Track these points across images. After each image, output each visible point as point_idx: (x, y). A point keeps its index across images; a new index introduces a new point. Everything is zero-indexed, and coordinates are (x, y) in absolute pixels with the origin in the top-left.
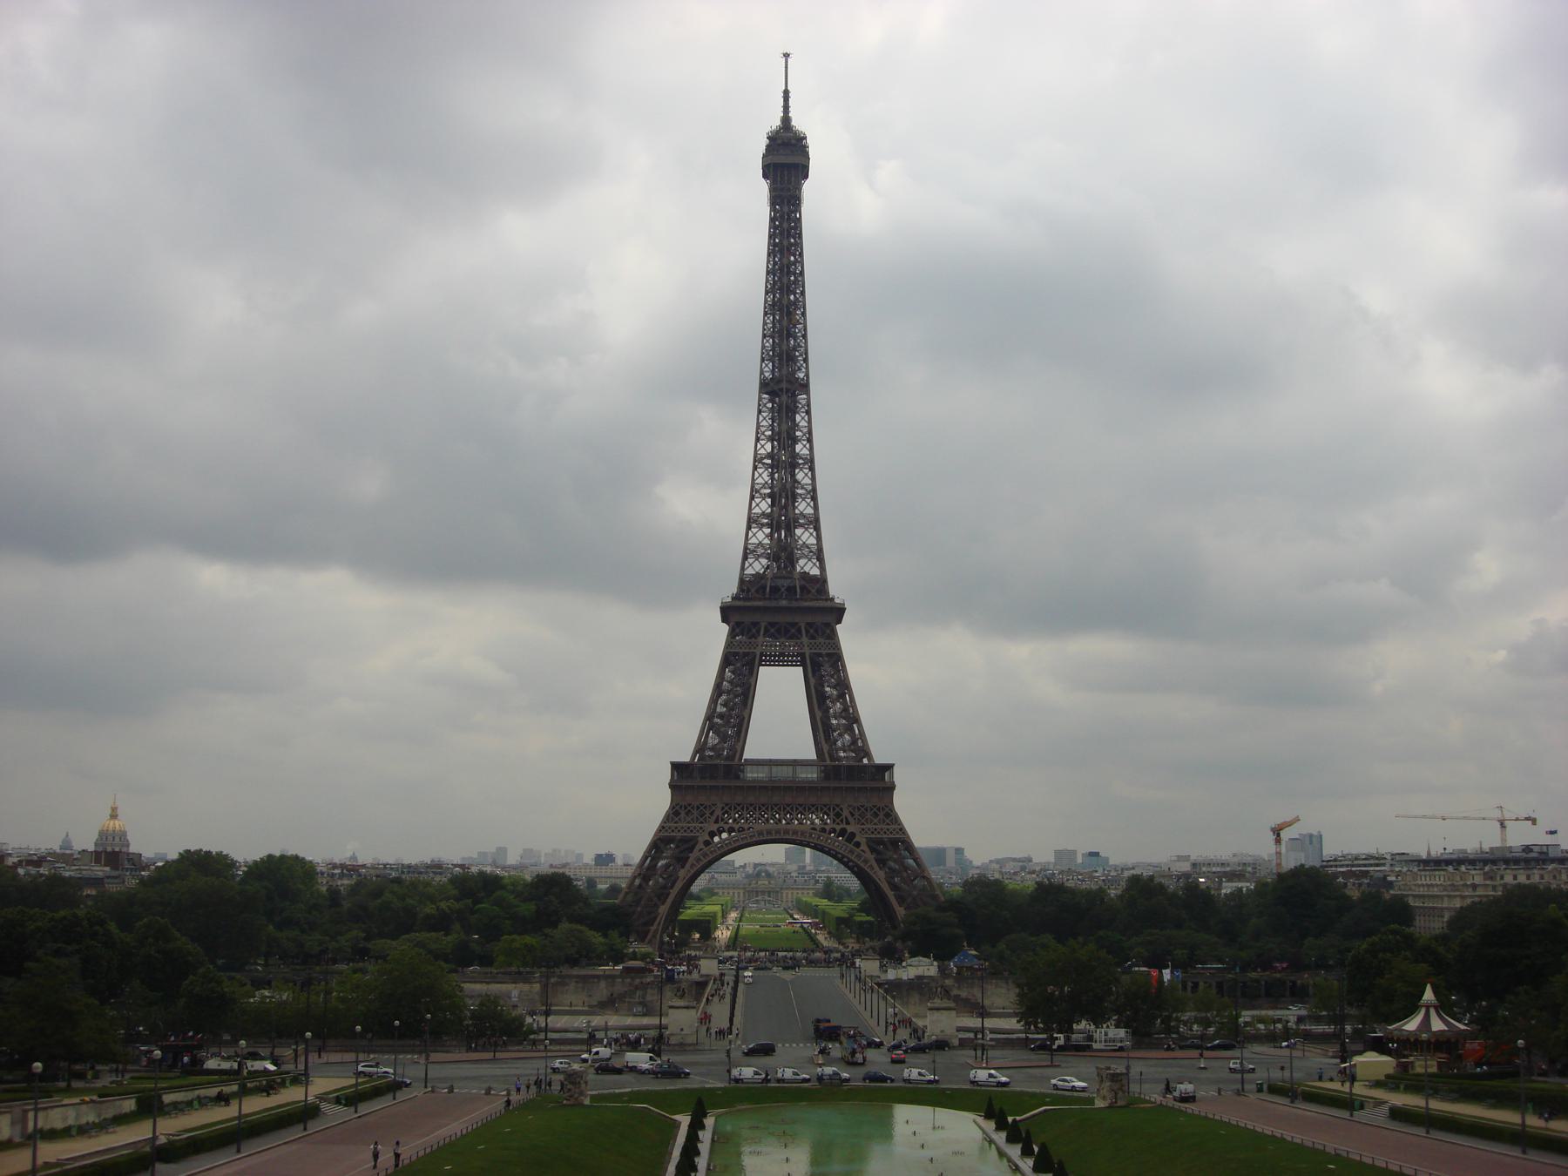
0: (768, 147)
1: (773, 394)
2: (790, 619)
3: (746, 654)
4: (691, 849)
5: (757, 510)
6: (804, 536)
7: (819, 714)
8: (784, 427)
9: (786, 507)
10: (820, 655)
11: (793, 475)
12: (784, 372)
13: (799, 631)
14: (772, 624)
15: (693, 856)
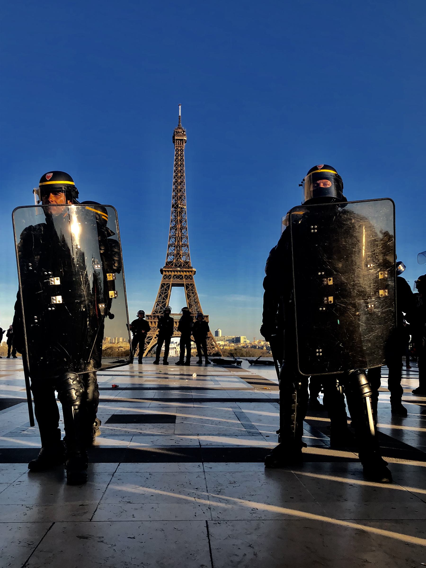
0: (174, 135)
1: (175, 208)
2: (179, 273)
3: (167, 284)
4: (151, 339)
5: (171, 243)
6: (184, 249)
7: (188, 301)
8: (179, 218)
9: (179, 242)
10: (188, 284)
11: (181, 232)
12: (179, 202)
13: (183, 277)
14: (175, 275)
15: (151, 341)
